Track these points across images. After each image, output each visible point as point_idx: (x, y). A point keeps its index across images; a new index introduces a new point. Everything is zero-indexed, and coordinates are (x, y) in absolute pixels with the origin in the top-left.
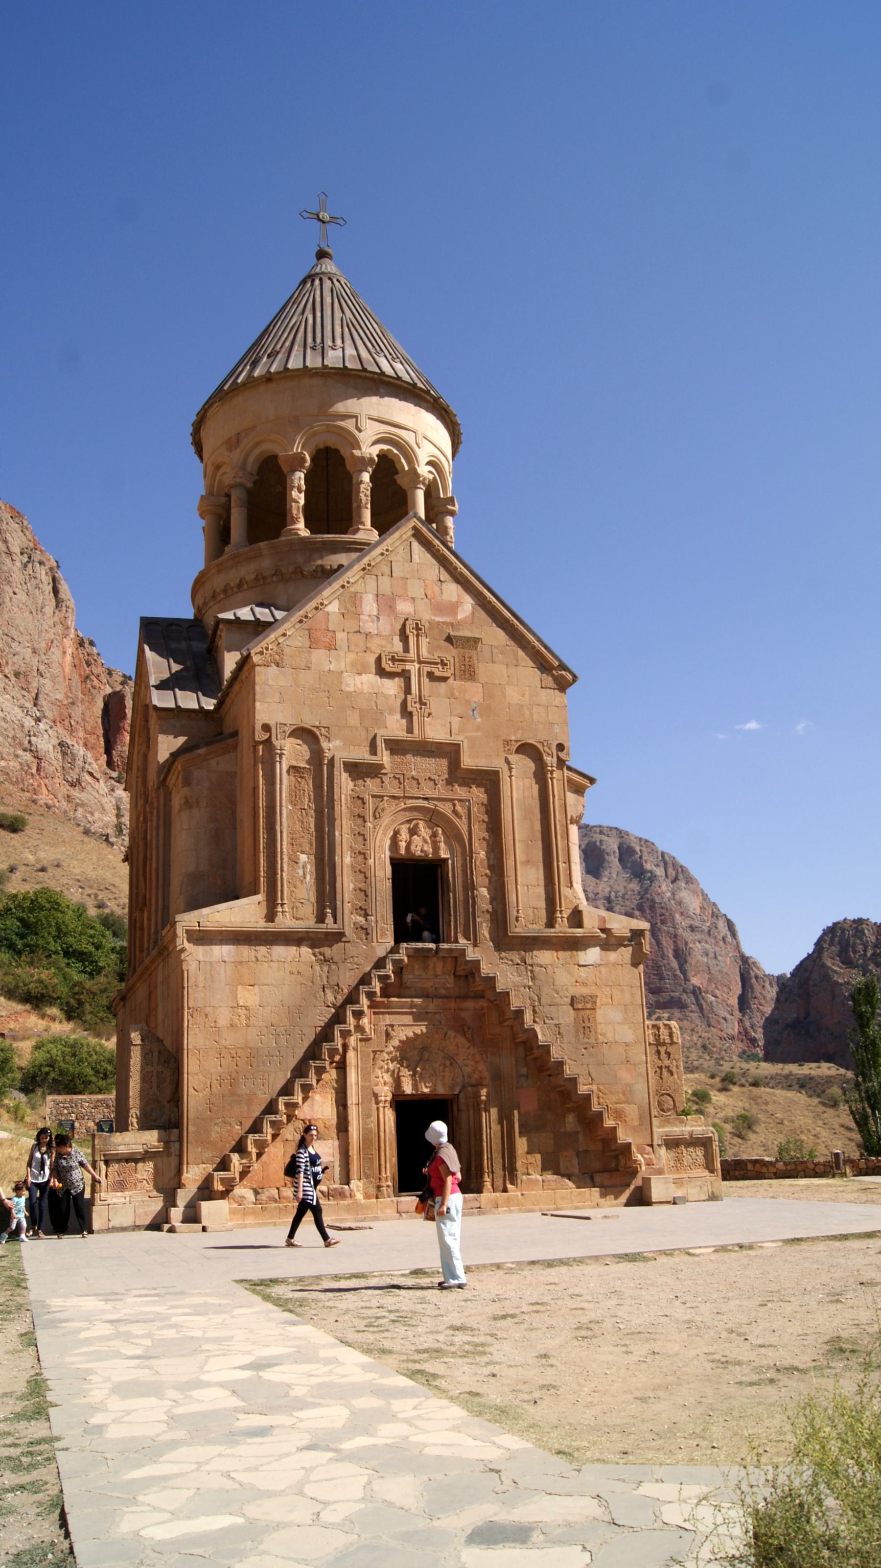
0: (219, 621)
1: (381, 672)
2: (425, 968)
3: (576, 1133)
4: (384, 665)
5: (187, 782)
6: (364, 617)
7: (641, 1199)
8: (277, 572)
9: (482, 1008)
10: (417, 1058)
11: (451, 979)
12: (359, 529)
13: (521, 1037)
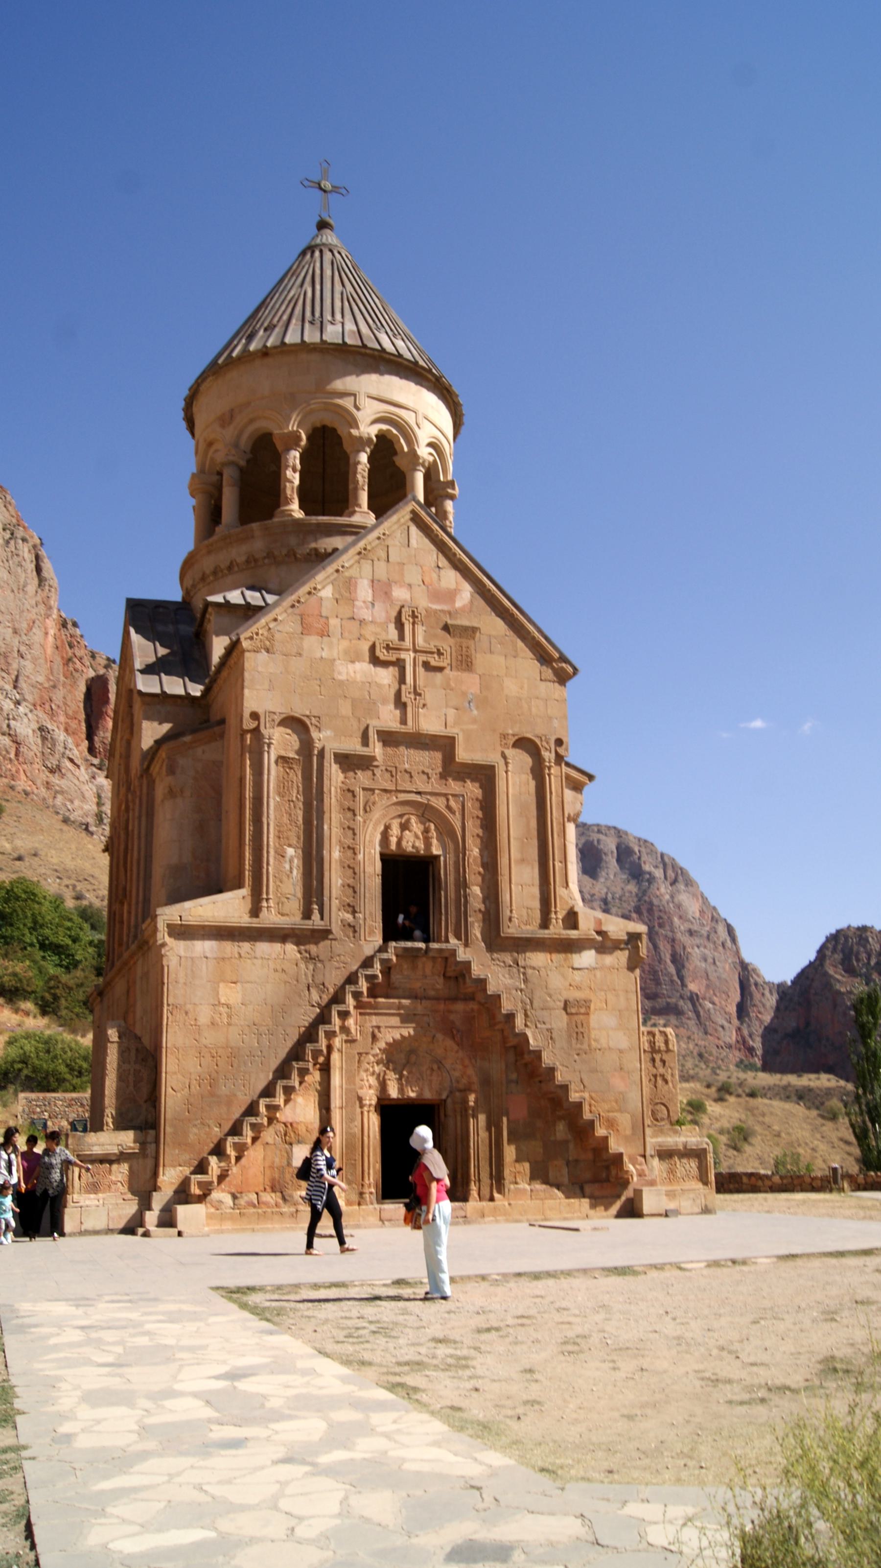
0: (208, 604)
1: (375, 661)
2: (414, 968)
3: (566, 1142)
5: (171, 771)
6: (358, 603)
7: (632, 1210)
8: (270, 555)
9: (472, 1010)
10: (404, 1061)
11: (441, 980)
12: (354, 512)
13: (512, 1042)
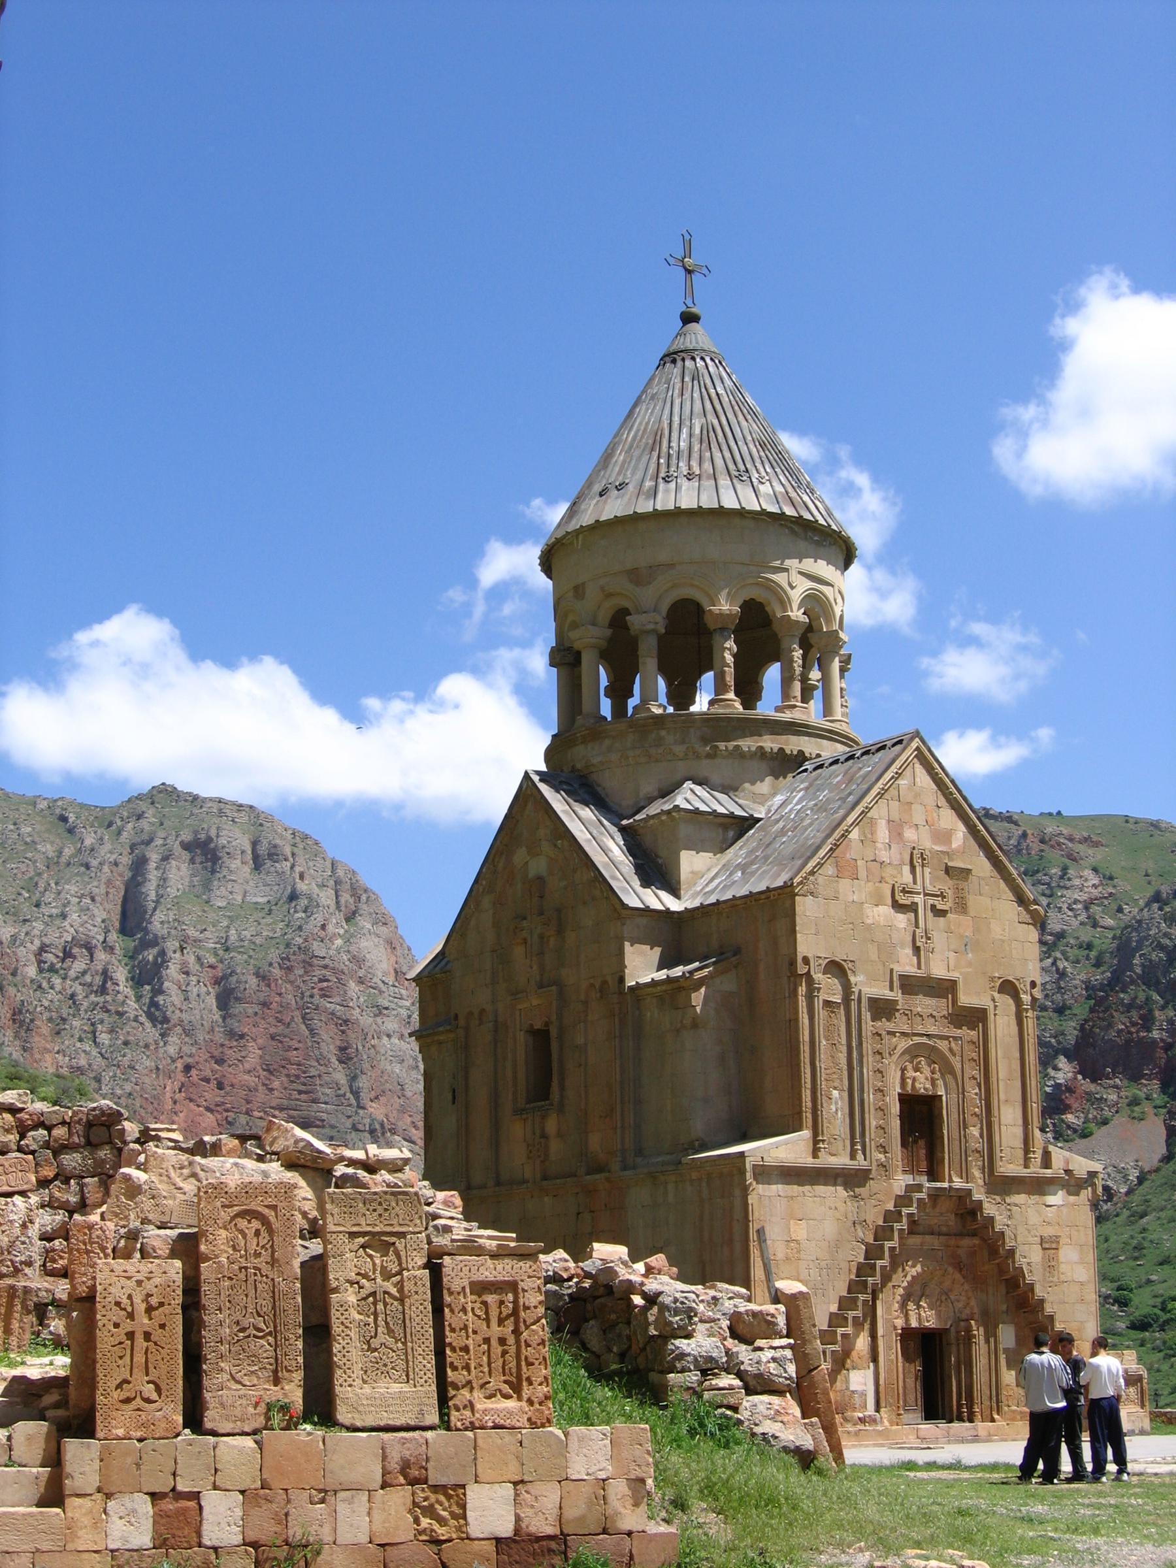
1: (897, 906)
4: (897, 898)
6: (879, 845)
